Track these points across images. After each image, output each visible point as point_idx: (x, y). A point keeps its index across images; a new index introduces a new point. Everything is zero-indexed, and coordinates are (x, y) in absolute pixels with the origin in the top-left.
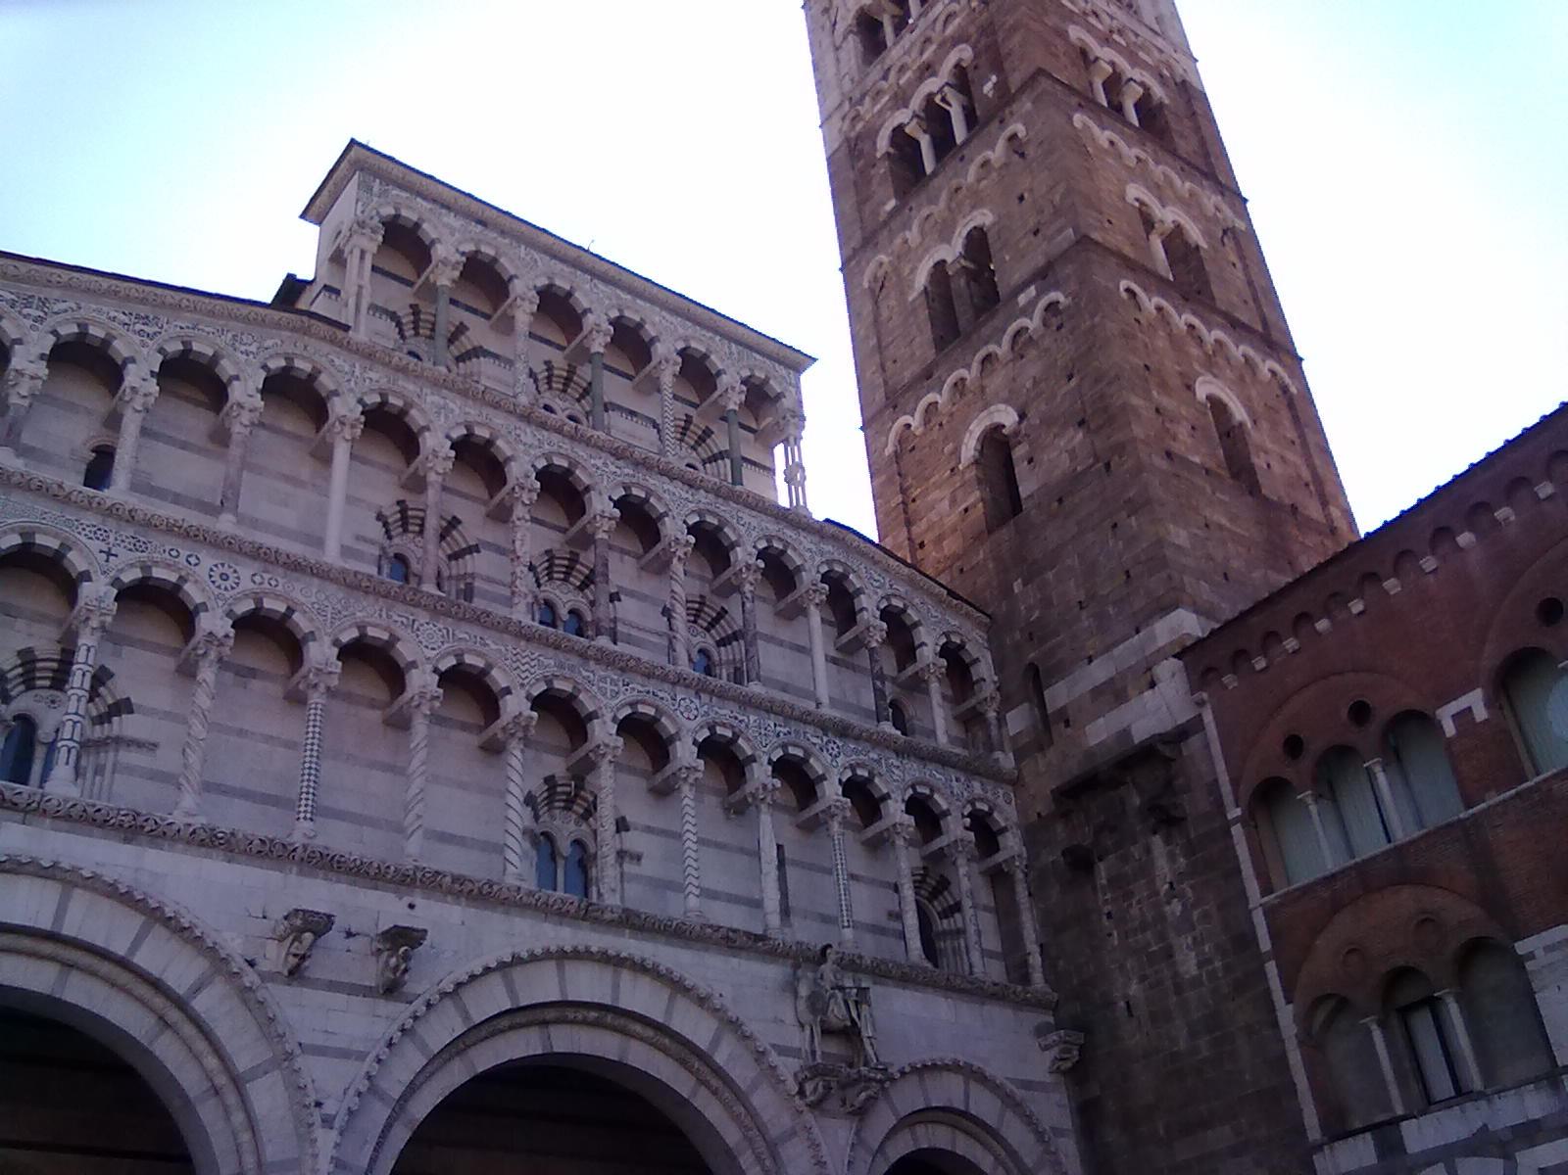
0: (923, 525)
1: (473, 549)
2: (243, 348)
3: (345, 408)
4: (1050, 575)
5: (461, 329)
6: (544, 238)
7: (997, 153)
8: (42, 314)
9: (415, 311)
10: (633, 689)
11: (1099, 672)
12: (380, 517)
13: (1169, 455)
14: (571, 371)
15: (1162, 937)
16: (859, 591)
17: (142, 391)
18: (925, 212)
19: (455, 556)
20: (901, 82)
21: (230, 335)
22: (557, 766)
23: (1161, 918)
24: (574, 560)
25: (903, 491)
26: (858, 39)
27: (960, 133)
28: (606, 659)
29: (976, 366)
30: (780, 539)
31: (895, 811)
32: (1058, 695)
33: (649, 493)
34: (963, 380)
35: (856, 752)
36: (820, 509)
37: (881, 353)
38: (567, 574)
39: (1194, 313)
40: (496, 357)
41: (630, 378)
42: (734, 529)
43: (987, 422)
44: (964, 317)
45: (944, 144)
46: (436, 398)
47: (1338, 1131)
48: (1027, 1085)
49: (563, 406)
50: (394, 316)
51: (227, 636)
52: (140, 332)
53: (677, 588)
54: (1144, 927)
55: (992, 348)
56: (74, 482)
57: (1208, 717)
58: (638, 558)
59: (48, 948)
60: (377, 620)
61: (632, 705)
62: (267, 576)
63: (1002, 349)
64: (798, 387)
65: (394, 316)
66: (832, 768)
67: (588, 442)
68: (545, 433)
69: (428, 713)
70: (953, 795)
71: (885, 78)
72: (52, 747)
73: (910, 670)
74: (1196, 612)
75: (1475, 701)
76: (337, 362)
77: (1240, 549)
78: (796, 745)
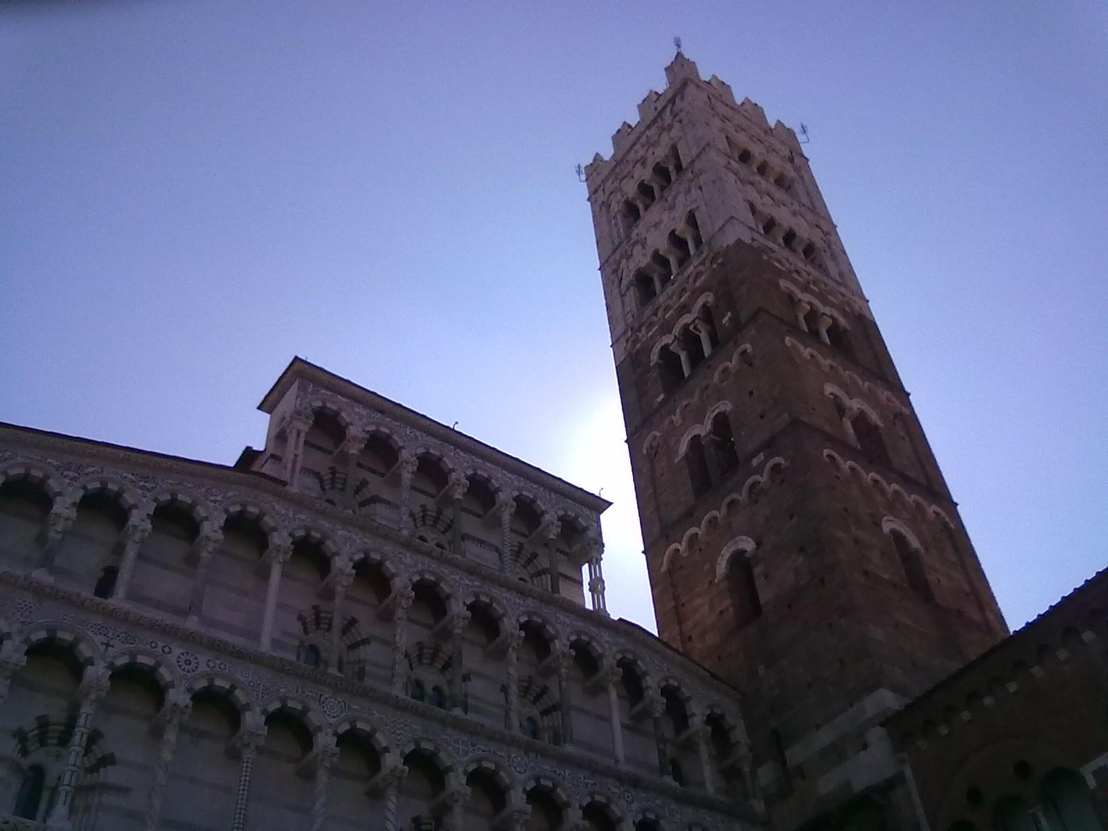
0: (688, 625)
1: (365, 642)
2: (212, 498)
3: (280, 540)
5: (364, 483)
6: (423, 421)
7: (733, 364)
8: (78, 476)
9: (333, 472)
10: (479, 749)
11: (825, 736)
12: (301, 618)
13: (866, 573)
14: (440, 512)
16: (645, 674)
17: (141, 528)
18: (685, 403)
19: (352, 647)
20: (666, 317)
21: (204, 489)
24: (437, 650)
25: (676, 598)
27: (707, 350)
28: (459, 725)
29: (724, 509)
30: (587, 634)
32: (796, 754)
33: (492, 599)
34: (715, 518)
36: (615, 612)
39: (878, 472)
41: (479, 516)
42: (554, 627)
43: (733, 548)
45: (696, 357)
46: (345, 533)
49: (432, 537)
50: (318, 475)
51: (187, 706)
52: (142, 488)
53: (512, 670)
55: (735, 496)
56: (88, 593)
57: (908, 772)
60: (294, 695)
61: (479, 761)
62: (218, 662)
63: (742, 496)
65: (318, 475)
67: (450, 563)
68: (419, 556)
69: (328, 766)
71: (655, 314)
72: (54, 791)
73: (684, 735)
76: (277, 507)
78: (600, 794)
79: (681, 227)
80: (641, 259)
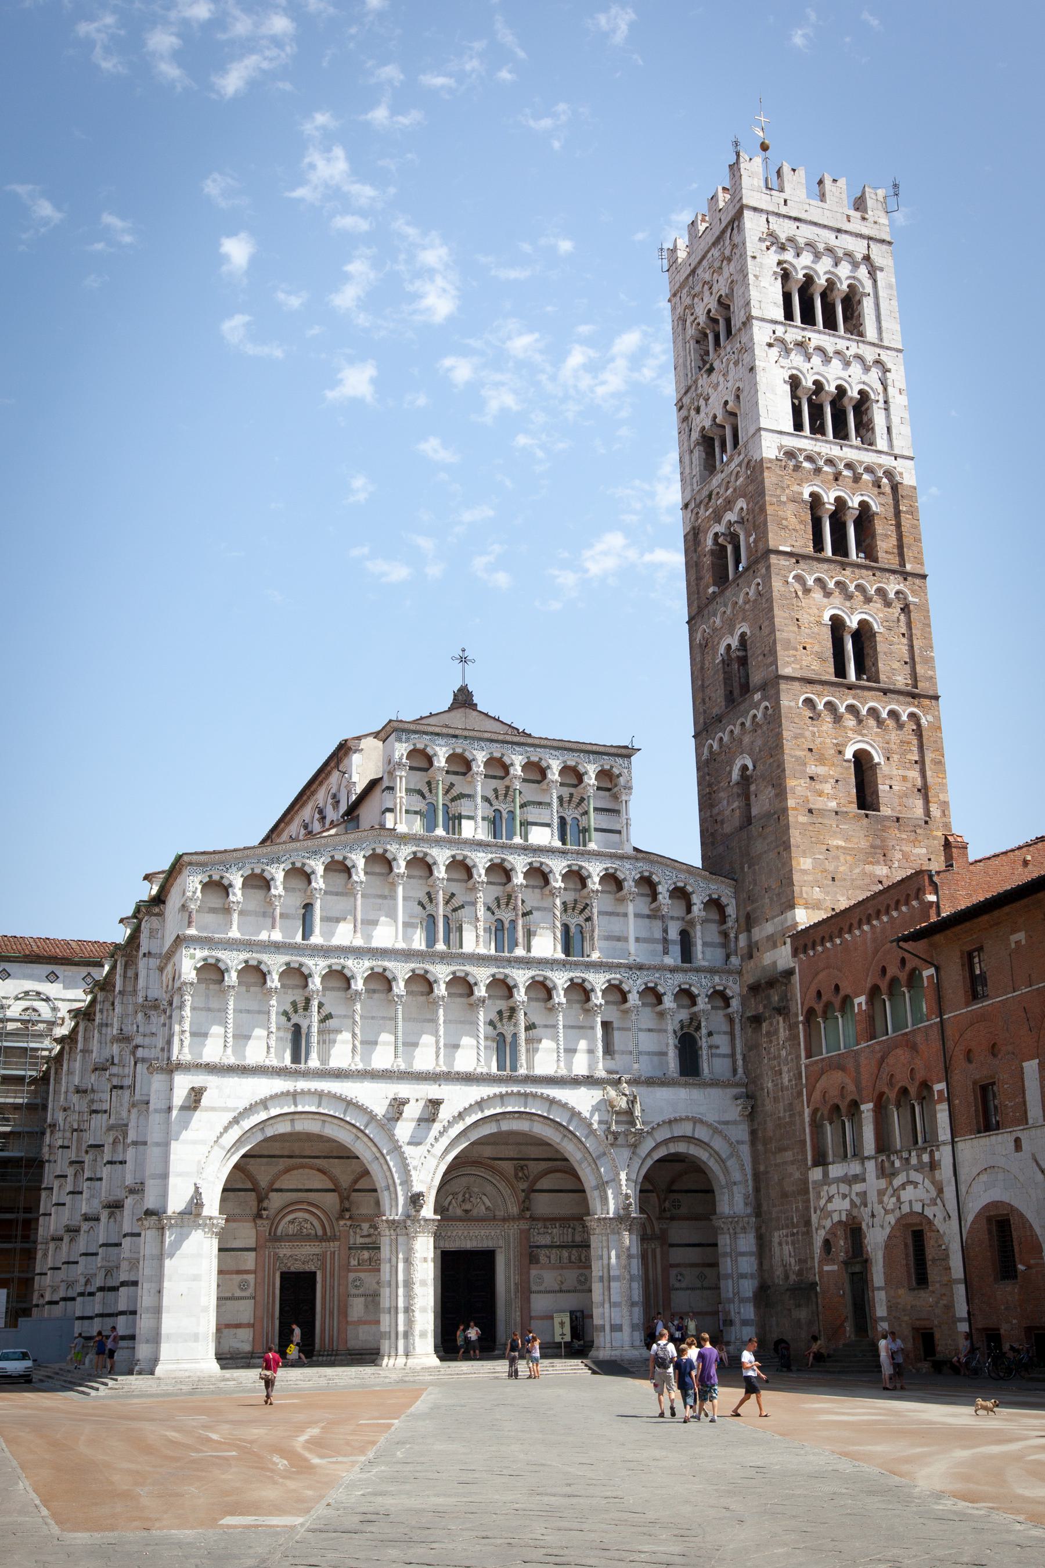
0: (715, 811)
1: (462, 907)
4: (757, 867)
5: (452, 785)
9: (429, 783)
12: (421, 904)
13: (810, 811)
14: (508, 788)
15: (779, 1065)
19: (455, 910)
22: (502, 1005)
23: (779, 1056)
26: (702, 448)
31: (668, 1002)
35: (649, 976)
37: (703, 691)
38: (507, 905)
39: (854, 698)
40: (469, 796)
41: (538, 782)
44: (737, 692)
47: (816, 1164)
48: (726, 1123)
54: (775, 1058)
58: (542, 888)
59: (317, 1117)
63: (748, 724)
64: (629, 768)
66: (634, 986)
70: (701, 986)
72: (308, 1035)
73: (689, 916)
74: (807, 908)
75: (862, 999)
77: (848, 858)
79: (731, 399)
80: (702, 420)
